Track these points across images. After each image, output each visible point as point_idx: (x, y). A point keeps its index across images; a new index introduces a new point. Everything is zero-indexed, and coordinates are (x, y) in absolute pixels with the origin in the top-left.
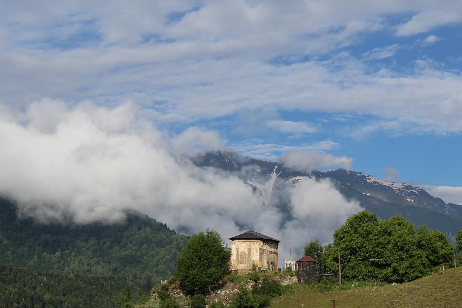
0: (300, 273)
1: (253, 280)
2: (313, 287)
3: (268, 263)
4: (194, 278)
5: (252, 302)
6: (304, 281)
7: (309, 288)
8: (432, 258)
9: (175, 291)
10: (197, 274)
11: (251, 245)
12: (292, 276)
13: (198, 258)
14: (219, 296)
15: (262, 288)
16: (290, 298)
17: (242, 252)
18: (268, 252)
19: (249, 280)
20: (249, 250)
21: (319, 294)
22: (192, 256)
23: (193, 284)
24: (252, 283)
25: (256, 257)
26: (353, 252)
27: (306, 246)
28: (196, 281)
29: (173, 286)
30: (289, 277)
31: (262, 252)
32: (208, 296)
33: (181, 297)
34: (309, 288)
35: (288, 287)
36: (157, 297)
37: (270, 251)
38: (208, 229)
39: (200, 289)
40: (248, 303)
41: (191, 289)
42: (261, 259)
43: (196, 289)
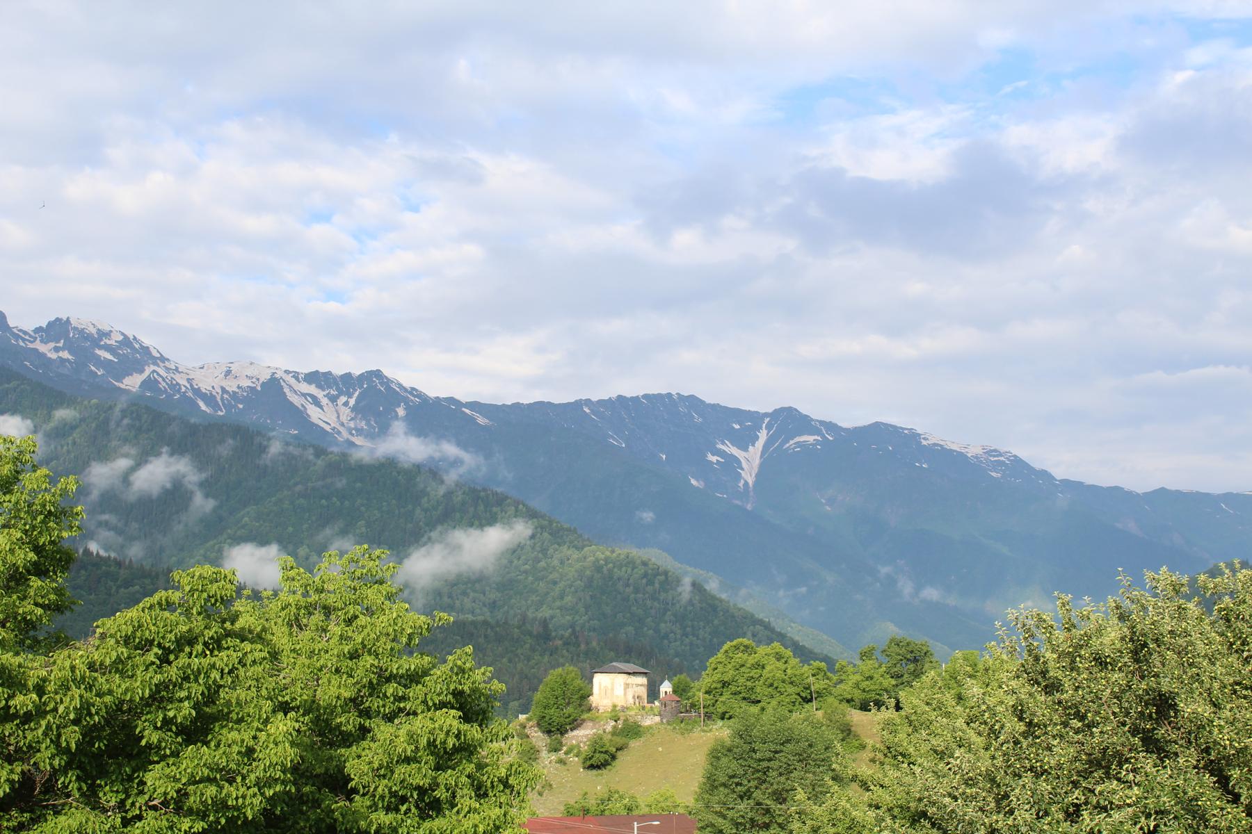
8: (803, 695)
21: (679, 736)
25: (619, 691)
26: (725, 684)
31: (627, 686)
35: (650, 727)
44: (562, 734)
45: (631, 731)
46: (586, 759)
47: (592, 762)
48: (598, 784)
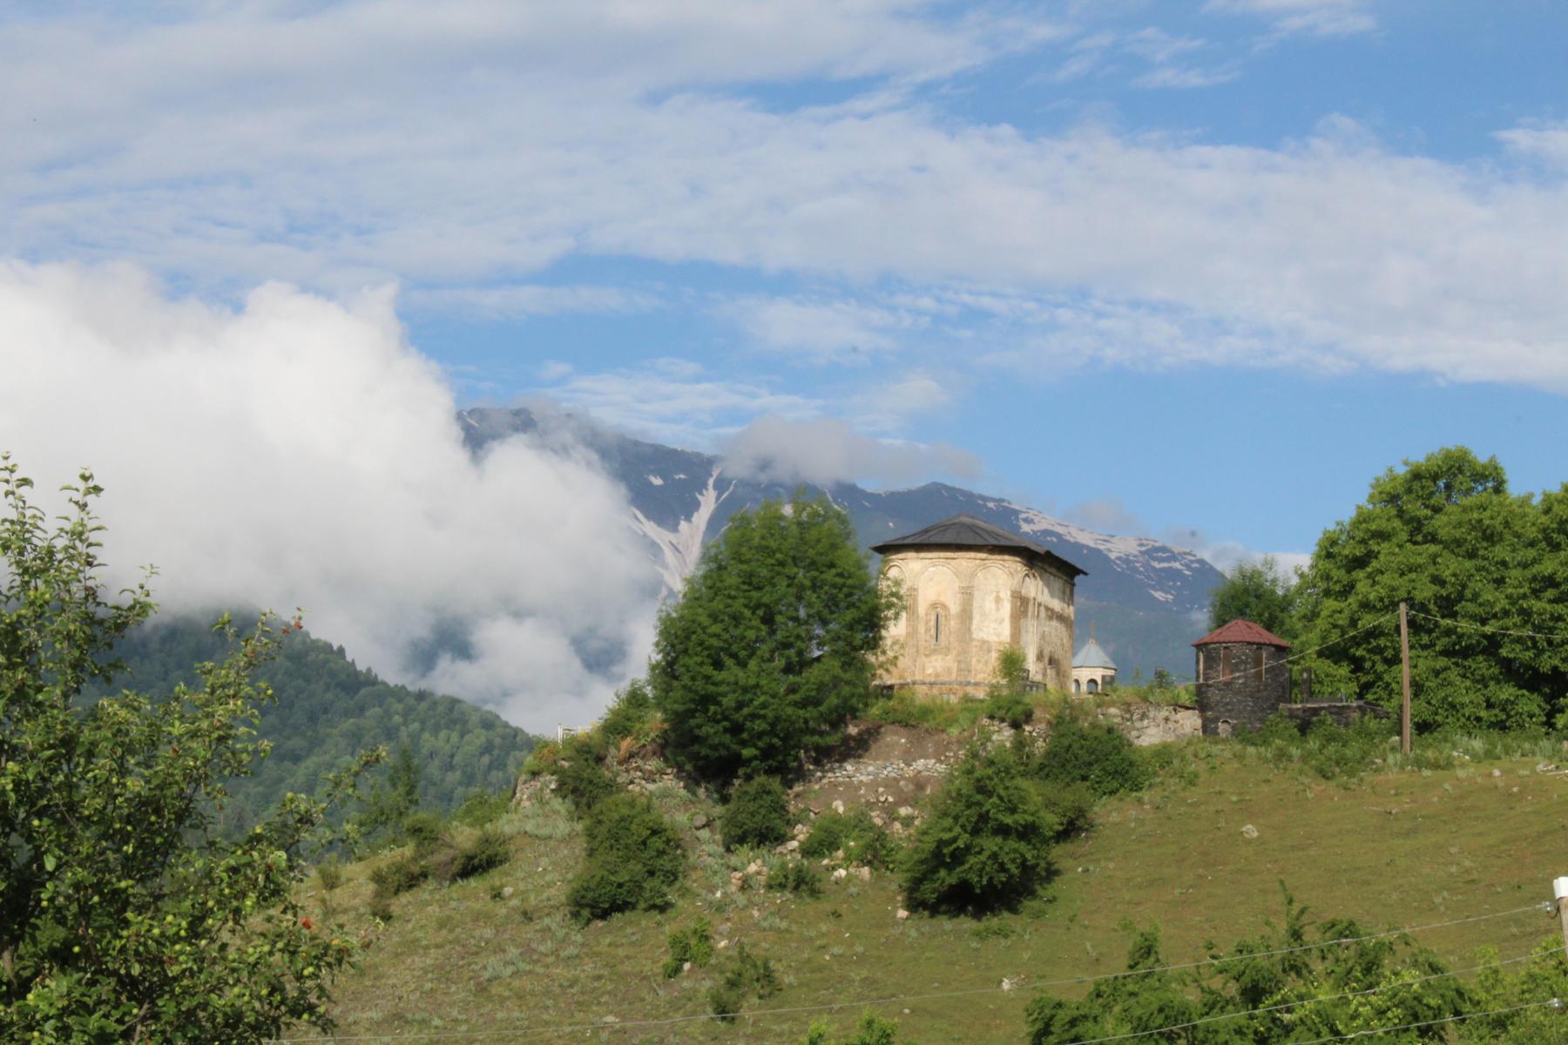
0: (1214, 696)
1: (1003, 720)
2: (1282, 755)
3: (1040, 657)
4: (740, 706)
5: (1033, 809)
6: (1236, 732)
7: (1267, 761)
9: (638, 769)
10: (757, 686)
11: (973, 575)
12: (1178, 706)
13: (760, 612)
14: (852, 788)
15: (1051, 754)
16: (1184, 800)
17: (934, 606)
18: (1043, 613)
19: (986, 721)
20: (968, 594)
22: (738, 605)
23: (736, 729)
28: (754, 716)
29: (626, 744)
30: (1164, 713)
31: (1022, 605)
32: (798, 788)
33: (666, 794)
34: (1267, 761)
35: (1163, 755)
36: (547, 794)
37: (1047, 609)
39: (767, 753)
40: (1013, 810)
41: (723, 752)
43: (747, 752)
44: (790, 774)
45: (1091, 758)
46: (916, 884)
47: (973, 870)
48: (1014, 966)
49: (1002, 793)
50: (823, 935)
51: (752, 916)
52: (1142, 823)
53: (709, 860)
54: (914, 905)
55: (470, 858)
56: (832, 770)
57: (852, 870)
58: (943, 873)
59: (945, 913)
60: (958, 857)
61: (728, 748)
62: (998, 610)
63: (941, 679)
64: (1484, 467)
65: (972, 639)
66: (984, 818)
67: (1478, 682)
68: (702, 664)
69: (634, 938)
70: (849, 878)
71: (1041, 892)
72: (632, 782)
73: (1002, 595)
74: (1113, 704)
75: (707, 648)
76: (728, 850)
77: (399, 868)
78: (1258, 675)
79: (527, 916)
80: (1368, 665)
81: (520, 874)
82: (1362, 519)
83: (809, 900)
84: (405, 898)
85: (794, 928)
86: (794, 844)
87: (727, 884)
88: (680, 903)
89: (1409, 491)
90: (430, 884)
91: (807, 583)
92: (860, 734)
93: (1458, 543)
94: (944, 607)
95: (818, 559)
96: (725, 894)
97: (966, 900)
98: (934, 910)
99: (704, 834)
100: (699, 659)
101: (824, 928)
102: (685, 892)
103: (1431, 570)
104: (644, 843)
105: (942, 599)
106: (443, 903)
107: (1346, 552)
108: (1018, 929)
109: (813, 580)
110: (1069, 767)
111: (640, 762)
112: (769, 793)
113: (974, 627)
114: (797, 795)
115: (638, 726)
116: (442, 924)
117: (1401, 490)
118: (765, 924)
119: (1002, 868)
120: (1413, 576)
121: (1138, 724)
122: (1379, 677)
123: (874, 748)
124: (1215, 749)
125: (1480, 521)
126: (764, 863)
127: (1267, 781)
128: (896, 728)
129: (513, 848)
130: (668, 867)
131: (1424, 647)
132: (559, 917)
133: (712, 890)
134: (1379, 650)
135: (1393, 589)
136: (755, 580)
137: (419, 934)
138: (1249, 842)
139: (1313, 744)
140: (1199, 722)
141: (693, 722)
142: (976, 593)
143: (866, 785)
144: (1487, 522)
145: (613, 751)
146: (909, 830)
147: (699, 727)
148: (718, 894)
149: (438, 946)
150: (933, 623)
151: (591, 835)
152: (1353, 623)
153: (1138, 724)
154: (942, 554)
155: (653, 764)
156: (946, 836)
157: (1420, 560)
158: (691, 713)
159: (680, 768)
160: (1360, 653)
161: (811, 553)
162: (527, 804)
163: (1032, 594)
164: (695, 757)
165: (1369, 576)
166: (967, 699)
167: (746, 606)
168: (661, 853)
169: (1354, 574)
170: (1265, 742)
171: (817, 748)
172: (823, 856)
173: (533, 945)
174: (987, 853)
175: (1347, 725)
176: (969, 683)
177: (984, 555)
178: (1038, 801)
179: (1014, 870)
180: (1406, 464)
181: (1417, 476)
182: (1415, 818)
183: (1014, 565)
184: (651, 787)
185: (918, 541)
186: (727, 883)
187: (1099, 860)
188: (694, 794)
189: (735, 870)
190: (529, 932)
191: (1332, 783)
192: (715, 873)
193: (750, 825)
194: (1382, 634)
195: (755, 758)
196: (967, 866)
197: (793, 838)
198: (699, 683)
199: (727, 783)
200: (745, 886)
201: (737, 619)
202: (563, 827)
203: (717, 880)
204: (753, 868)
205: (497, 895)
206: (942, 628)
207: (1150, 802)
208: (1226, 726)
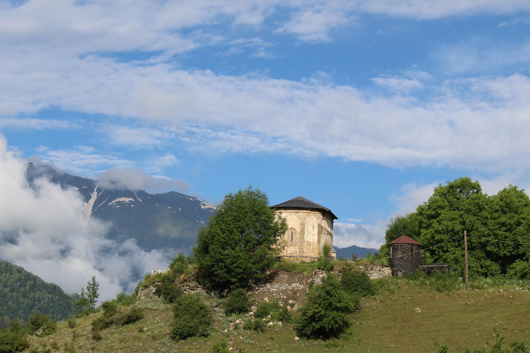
0: (396, 262)
1: (323, 270)
4: (233, 263)
6: (405, 275)
7: (418, 285)
10: (239, 256)
11: (305, 218)
12: (383, 266)
13: (239, 230)
15: (343, 282)
19: (317, 270)
20: (303, 225)
21: (438, 295)
23: (229, 271)
24: (323, 275)
27: (390, 223)
28: (237, 267)
30: (379, 268)
32: (250, 293)
33: (198, 294)
34: (418, 285)
35: (381, 283)
36: (151, 294)
37: (327, 231)
38: (250, 188)
40: (340, 302)
42: (319, 241)
43: (233, 280)
47: (326, 323)
49: (336, 295)
50: (268, 346)
51: (240, 339)
52: (377, 306)
53: (221, 319)
54: (302, 334)
55: (130, 317)
56: (262, 287)
57: (275, 322)
58: (314, 324)
59: (312, 338)
60: (321, 318)
61: (226, 279)
62: (313, 231)
63: (293, 255)
64: (474, 184)
65: (304, 241)
66: (330, 304)
67: (477, 259)
68: (219, 248)
69: (197, 346)
70: (274, 326)
71: (346, 331)
72: (185, 290)
73: (315, 225)
74: (361, 265)
75: (220, 242)
76: (227, 315)
77: (100, 320)
78: (412, 255)
79: (154, 338)
80: (437, 252)
81: (148, 323)
82: (432, 201)
83: (260, 333)
84: (105, 331)
85: (257, 343)
86: (252, 313)
87: (228, 326)
88: (212, 334)
89: (448, 192)
90: (114, 326)
91: (255, 220)
92: (271, 274)
93: (470, 210)
94: (295, 229)
95: (259, 211)
96: (228, 331)
97: (322, 334)
98: (308, 337)
99: (217, 309)
100: (217, 246)
101: (269, 343)
102: (213, 330)
103: (460, 220)
104: (198, 312)
105: (294, 227)
106: (120, 333)
107: (429, 212)
108: (342, 344)
109: (258, 219)
110: (350, 286)
111: (188, 283)
112: (243, 294)
113: (305, 237)
114: (249, 295)
115: (186, 270)
116: (121, 341)
117: (446, 191)
118: (246, 342)
119: (336, 322)
120: (454, 222)
121: (370, 272)
122: (441, 257)
123: (276, 279)
124: (399, 281)
125: (478, 203)
126: (242, 320)
127: (420, 292)
128: (284, 272)
129: (144, 314)
130: (207, 321)
131: (456, 247)
132: (167, 339)
133: (224, 329)
134: (442, 247)
135: (448, 226)
136: (237, 218)
137: (113, 344)
138: (418, 314)
139: (433, 280)
140: (391, 271)
141: (214, 269)
142: (306, 225)
143: (275, 292)
144: (481, 203)
145: (177, 279)
146: (295, 308)
147: (216, 271)
148: (226, 331)
149: (121, 349)
150: (290, 235)
151: (177, 309)
152: (433, 238)
153: (370, 272)
154: (294, 211)
155: (193, 284)
156: (317, 311)
157: (456, 216)
158: (213, 266)
159: (204, 285)
160: (435, 248)
161: (256, 209)
162: (143, 297)
163: (323, 226)
164: (211, 281)
165: (438, 221)
166: (303, 262)
167: (234, 227)
168: (204, 316)
169: (431, 221)
170: (416, 279)
171: (255, 279)
172: (263, 317)
173: (159, 349)
174: (331, 317)
175: (444, 273)
176: (303, 257)
177: (309, 212)
178: (347, 298)
179: (341, 324)
180: (448, 183)
181: (451, 187)
182: (477, 306)
183: (319, 215)
184: (193, 292)
185: (285, 206)
186: (229, 327)
187: (364, 320)
188: (210, 295)
189: (231, 322)
190: (156, 344)
191: (442, 293)
192: (224, 323)
193: (236, 306)
194: (443, 242)
195: (236, 282)
196: (324, 322)
197: (251, 311)
198: (218, 254)
199: (223, 291)
200: (236, 327)
201: (231, 232)
202: (162, 306)
203: (225, 326)
204: (238, 321)
205: (141, 331)
206: (293, 237)
207: (379, 300)
208: (401, 273)
